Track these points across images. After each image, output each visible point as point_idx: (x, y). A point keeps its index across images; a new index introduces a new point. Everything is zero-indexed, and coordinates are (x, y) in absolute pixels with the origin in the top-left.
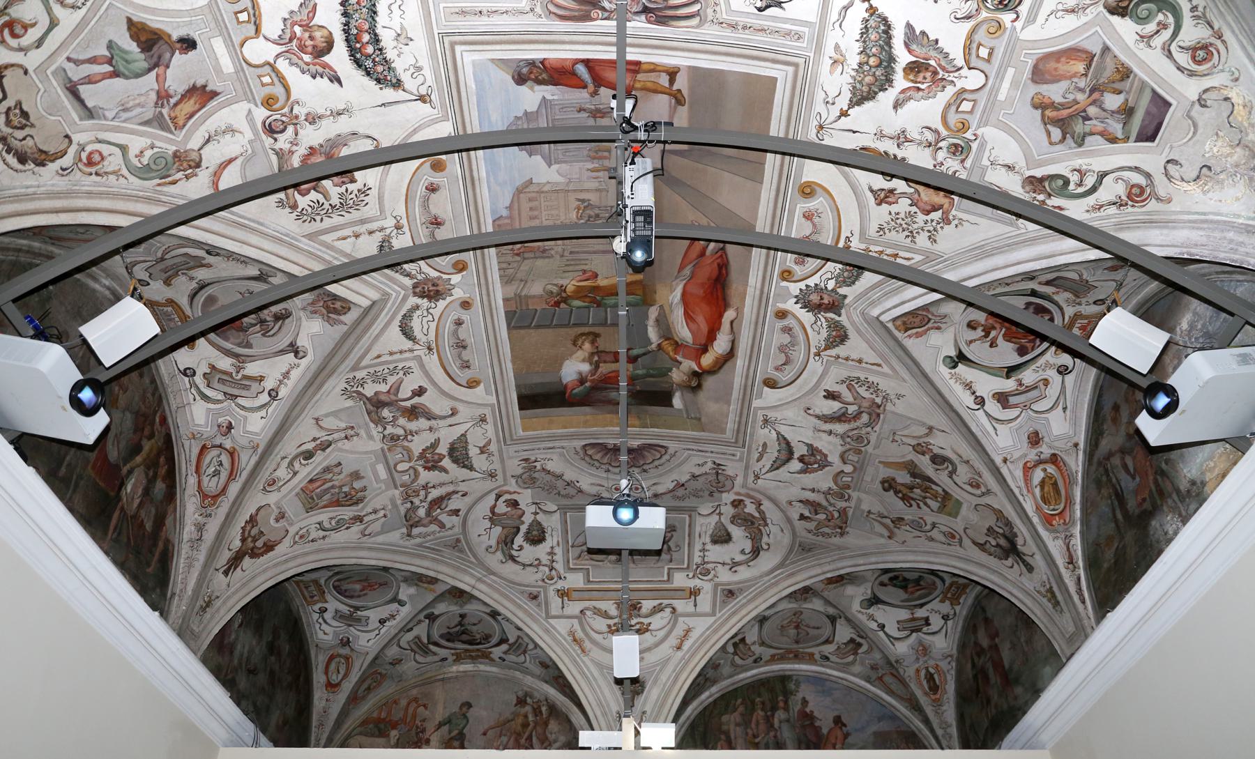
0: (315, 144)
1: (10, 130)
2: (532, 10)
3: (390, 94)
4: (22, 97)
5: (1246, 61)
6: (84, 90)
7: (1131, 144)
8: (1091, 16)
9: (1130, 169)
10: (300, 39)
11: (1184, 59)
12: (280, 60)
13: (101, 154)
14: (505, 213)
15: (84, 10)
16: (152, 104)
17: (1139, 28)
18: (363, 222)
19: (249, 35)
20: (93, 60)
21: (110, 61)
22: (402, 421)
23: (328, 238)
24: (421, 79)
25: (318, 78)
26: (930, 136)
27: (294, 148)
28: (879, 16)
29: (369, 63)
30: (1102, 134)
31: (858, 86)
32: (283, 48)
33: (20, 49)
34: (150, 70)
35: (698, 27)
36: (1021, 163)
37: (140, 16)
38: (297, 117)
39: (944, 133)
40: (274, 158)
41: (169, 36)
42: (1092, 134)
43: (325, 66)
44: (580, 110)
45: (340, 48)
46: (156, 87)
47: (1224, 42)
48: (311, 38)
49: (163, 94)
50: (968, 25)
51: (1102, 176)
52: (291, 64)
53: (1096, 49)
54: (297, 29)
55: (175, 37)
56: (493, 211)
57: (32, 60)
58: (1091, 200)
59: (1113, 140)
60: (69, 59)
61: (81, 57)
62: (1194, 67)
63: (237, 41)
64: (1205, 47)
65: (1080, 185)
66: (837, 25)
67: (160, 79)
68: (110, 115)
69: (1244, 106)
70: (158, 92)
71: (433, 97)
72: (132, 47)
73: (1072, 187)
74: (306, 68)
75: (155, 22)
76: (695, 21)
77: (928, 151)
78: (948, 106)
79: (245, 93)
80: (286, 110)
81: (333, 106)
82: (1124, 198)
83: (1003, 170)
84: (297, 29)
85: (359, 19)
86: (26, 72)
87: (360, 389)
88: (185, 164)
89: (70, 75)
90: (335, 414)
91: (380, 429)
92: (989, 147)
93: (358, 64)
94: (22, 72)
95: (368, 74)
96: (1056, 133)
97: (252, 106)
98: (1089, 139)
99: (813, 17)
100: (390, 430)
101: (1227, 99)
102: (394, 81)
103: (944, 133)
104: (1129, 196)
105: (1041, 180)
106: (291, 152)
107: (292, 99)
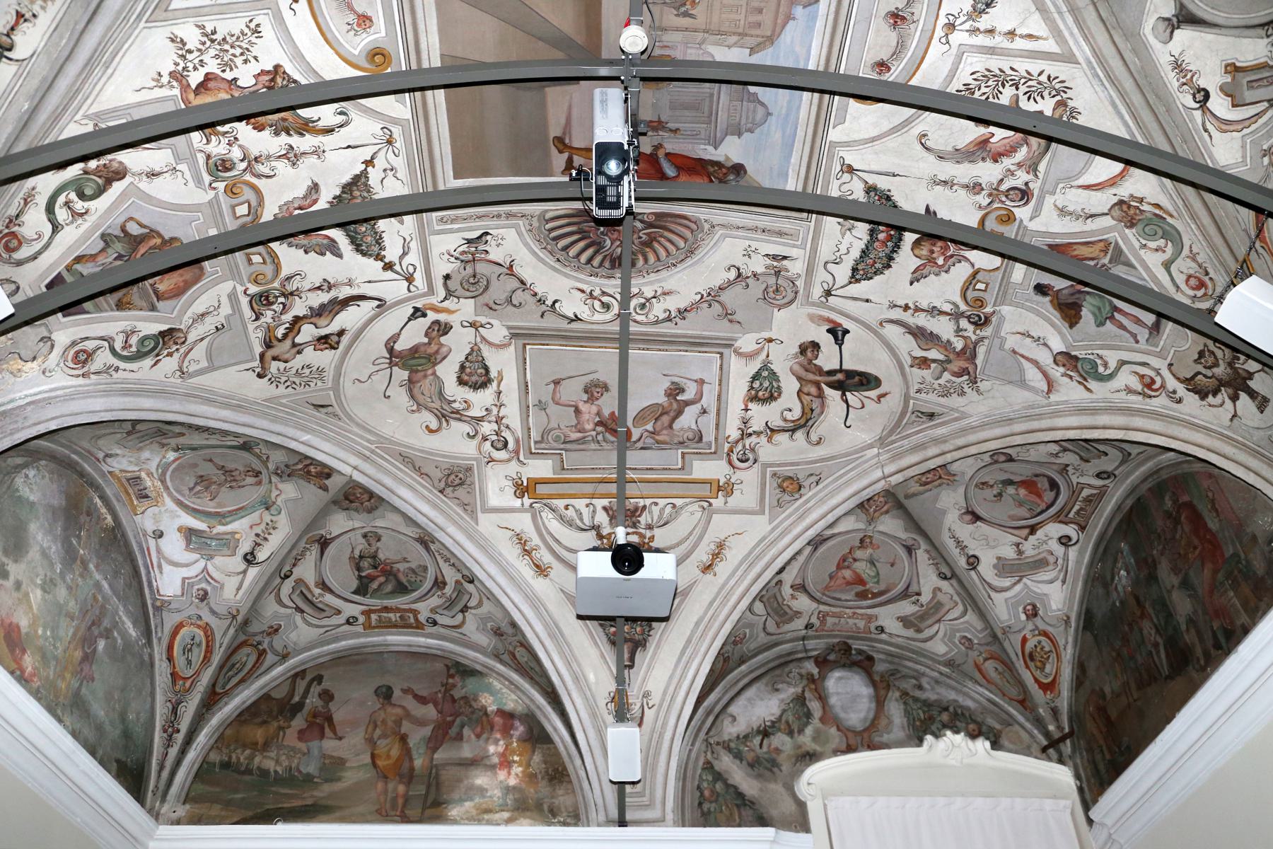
0: (989, 164)
1: (1221, 362)
2: (713, 227)
3: (883, 183)
5: (53, 386)
7: (61, 268)
8: (186, 318)
9: (39, 253)
10: (943, 254)
11: (90, 345)
13: (1187, 281)
14: (799, 11)
17: (141, 335)
18: (991, 51)
21: (1112, 318)
23: (1051, 46)
24: (844, 188)
26: (261, 168)
27: (1013, 168)
28: (371, 255)
30: (93, 257)
31: (365, 194)
35: (547, 211)
36: (144, 185)
37: (1063, 326)
38: (990, 195)
39: (248, 177)
40: (1042, 167)
41: (1051, 302)
42: (103, 250)
44: (676, 131)
47: (78, 376)
48: (932, 252)
50: (285, 272)
51: (56, 228)
53: (160, 305)
54: (940, 261)
55: (1048, 299)
56: (813, 18)
58: (42, 201)
59: (79, 259)
60: (1137, 342)
61: (1128, 335)
62: (77, 348)
63: (999, 274)
64: (85, 362)
65: (67, 204)
66: (408, 239)
69: (19, 370)
71: (839, 168)
72: (1085, 312)
73: (73, 196)
75: (1055, 316)
76: (548, 216)
77: (254, 152)
78: (261, 202)
80: (996, 205)
81: (947, 192)
82: (15, 229)
83: (158, 169)
84: (940, 261)
88: (1132, 212)
92: (191, 184)
96: (134, 229)
97: (1025, 223)
98: (101, 245)
99: (434, 240)
101: (34, 358)
102: (872, 194)
103: (248, 177)
104: (13, 234)
105: (109, 182)
106: (1019, 165)
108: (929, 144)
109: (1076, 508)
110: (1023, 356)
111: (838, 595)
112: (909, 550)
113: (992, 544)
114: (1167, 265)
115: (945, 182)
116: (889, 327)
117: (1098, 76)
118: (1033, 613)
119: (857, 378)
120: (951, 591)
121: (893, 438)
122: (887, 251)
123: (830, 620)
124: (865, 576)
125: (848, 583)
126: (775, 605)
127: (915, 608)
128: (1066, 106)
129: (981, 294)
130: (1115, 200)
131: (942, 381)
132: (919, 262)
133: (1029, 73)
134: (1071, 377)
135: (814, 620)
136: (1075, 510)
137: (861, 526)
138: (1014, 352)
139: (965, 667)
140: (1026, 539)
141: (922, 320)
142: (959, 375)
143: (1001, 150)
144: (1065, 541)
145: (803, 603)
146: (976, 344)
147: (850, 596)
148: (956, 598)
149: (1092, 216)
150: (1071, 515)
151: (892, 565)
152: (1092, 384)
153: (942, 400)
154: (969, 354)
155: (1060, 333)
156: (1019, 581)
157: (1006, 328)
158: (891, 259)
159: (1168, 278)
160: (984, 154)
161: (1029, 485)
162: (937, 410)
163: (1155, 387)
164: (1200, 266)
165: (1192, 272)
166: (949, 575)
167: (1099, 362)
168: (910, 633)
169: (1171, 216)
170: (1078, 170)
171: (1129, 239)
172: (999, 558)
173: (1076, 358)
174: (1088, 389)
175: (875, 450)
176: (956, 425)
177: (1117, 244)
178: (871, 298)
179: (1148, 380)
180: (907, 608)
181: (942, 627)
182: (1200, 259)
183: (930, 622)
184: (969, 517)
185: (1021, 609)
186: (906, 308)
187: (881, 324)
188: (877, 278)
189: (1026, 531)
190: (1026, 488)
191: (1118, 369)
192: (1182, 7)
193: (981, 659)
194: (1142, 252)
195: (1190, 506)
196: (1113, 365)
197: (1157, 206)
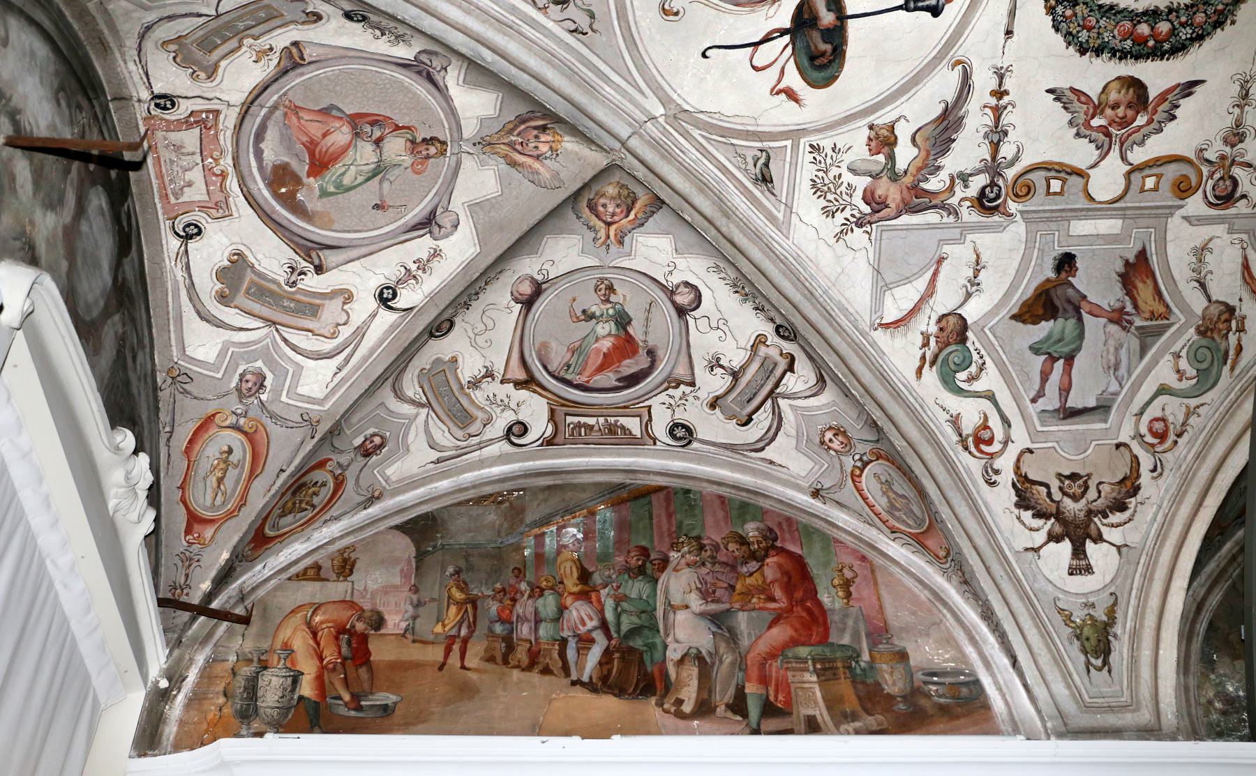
6: (1074, 401)
12: (1131, 157)
15: (987, 359)
16: (1123, 334)
19: (1081, 187)
21: (1056, 360)
25: (1177, 112)
29: (1185, 33)
33: (1005, 443)
34: (1080, 319)
37: (1014, 304)
38: (1223, 158)
41: (1048, 280)
43: (1163, 97)
48: (1115, 106)
49: (1115, 315)
52: (1142, 143)
54: (1096, 122)
55: (1052, 275)
57: (1021, 438)
60: (1034, 401)
61: (1037, 387)
63: (1082, 203)
67: (1096, 312)
68: (1114, 387)
70: (1111, 321)
72: (1045, 327)
74: (1154, 125)
75: (1026, 290)
79: (1157, 216)
81: (1229, 102)
84: (1096, 122)
85: (1112, 33)
86: (1030, 451)
93: (1179, 49)
94: (1027, 455)
95: (1200, 38)
97: (1182, 212)
107: (1192, 156)
109: (591, 421)
110: (935, 274)
111: (271, 135)
112: (428, 223)
113: (480, 340)
114: (1163, 390)
116: (955, 77)
118: (366, 452)
119: (828, 47)
120: (358, 318)
121: (696, 133)
122: (1116, 43)
123: (190, 138)
124: (338, 168)
125: (311, 146)
126: (241, 25)
127: (281, 275)
129: (1041, 189)
130: (1233, 302)
131: (848, 177)
132: (1094, 94)
134: (926, 344)
135: (184, 108)
136: (583, 420)
137: (469, 130)
138: (940, 261)
139: (188, 401)
140: (502, 382)
141: (976, 119)
142: (869, 197)
144: (517, 430)
145: (241, 74)
146: (943, 206)
147: (272, 152)
148: (346, 332)
149: (1203, 286)
150: (569, 419)
151: (377, 207)
152: (931, 375)
153: (804, 187)
154: (917, 200)
155: (997, 307)
156: (422, 405)
157: (985, 241)
158: (1098, 52)
159: (1147, 398)
161: (626, 345)
162: (781, 185)
163: (983, 447)
164: (1183, 424)
165: (1171, 419)
166: (400, 303)
167: (973, 369)
168: (207, 285)
169: (1232, 369)
171: (1181, 335)
172: (454, 360)
173: (963, 339)
174: (919, 372)
175: (662, 111)
176: (760, 222)
177: (1169, 326)
178: (1015, 38)
179: (986, 435)
180: (271, 257)
181: (259, 333)
182: (1193, 420)
183: (257, 308)
184: (527, 289)
185: (371, 431)
186: (999, 94)
187: (959, 62)
188: (1059, 38)
189: (521, 376)
190: (615, 347)
191: (977, 395)
193: (232, 420)
194: (1171, 358)
195: (799, 562)
196: (978, 386)
197: (1239, 349)
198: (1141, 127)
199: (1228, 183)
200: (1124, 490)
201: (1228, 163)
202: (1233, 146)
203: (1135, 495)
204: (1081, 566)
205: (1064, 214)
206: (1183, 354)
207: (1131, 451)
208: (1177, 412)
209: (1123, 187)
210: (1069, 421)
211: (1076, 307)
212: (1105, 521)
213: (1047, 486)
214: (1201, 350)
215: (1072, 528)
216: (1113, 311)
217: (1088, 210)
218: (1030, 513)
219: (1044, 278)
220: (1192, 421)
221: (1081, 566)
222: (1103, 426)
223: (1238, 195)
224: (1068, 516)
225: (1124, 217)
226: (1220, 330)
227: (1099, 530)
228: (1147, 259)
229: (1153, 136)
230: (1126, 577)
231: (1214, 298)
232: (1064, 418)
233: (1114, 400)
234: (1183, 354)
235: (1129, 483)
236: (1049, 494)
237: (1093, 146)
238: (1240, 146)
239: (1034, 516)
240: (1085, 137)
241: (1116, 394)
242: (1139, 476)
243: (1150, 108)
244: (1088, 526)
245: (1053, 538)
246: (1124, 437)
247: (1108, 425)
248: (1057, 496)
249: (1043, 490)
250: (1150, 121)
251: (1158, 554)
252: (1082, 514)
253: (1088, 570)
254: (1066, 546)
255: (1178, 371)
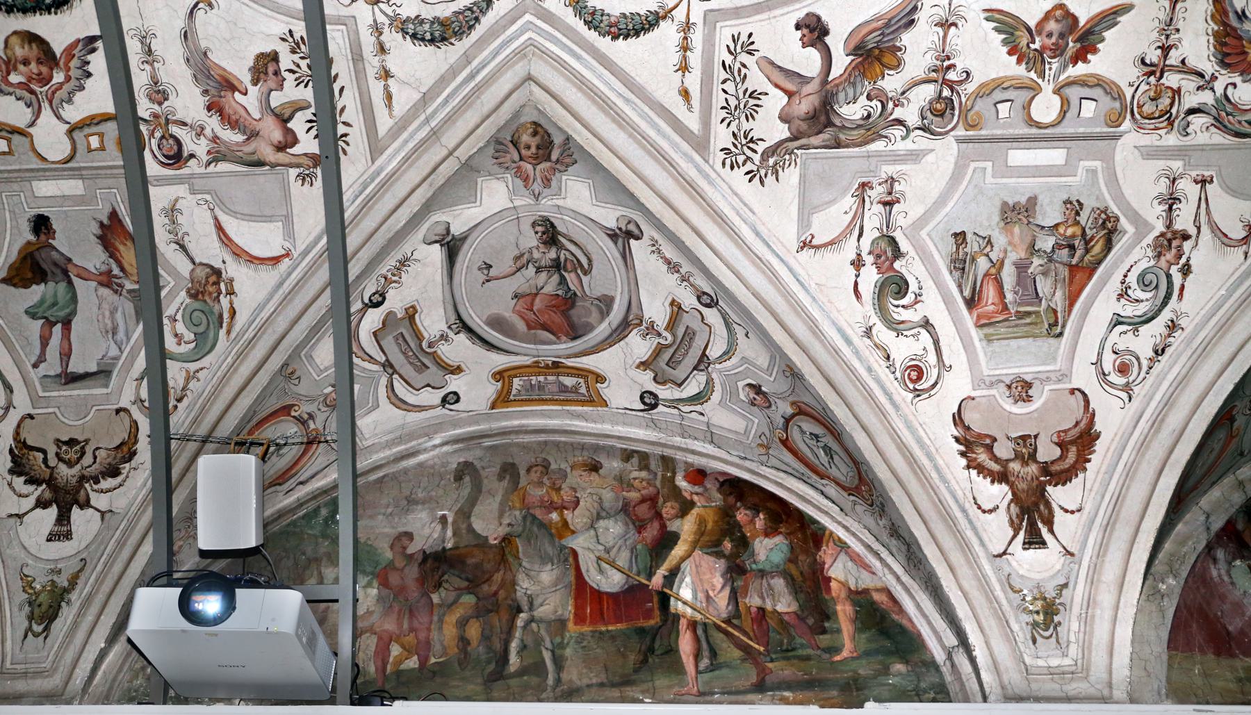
0: (201, 101)
4: (52, 436)
6: (76, 366)
10: (30, 79)
16: (116, 297)
18: (357, 58)
19: (28, 146)
20: (45, 341)
22: (891, 83)
23: (384, 123)
27: (208, 132)
32: (45, 105)
34: (70, 283)
40: (223, 167)
41: (29, 243)
45: (39, 24)
46: (94, 284)
49: (104, 279)
52: (70, 101)
55: (32, 238)
57: (22, 403)
60: (35, 366)
61: (38, 352)
63: (36, 164)
67: (85, 275)
68: (114, 351)
70: (101, 284)
72: (36, 292)
74: (73, 83)
84: (14, 78)
86: (31, 417)
87: (761, 147)
88: (211, 289)
89: (52, 373)
90: (806, 213)
91: (898, 132)
94: (28, 421)
100: (910, 114)
106: (215, 139)
108: (200, 14)
115: (150, 52)
117: (365, 189)
128: (315, 167)
130: (217, 264)
133: (342, 110)
143: (228, 110)
149: (183, 247)
160: (213, 91)
169: (229, 332)
170: (238, 209)
192: (463, 238)
197: (233, 312)
198: (61, 85)
199: (171, 141)
200: (119, 455)
201: (163, 121)
202: (160, 104)
203: (130, 460)
204: (61, 532)
205: (22, 175)
206: (179, 317)
207: (130, 416)
208: (177, 377)
209: (69, 147)
210: (71, 386)
211: (63, 270)
212: (95, 487)
213: (44, 452)
214: (196, 313)
215: (62, 494)
216: (101, 274)
217: (45, 170)
218: (22, 479)
219: (25, 241)
220: (191, 385)
221: (61, 532)
222: (104, 391)
223: (185, 154)
224: (61, 482)
225: (82, 177)
226: (210, 294)
227: (88, 495)
228: (120, 221)
229: (78, 94)
230: (102, 543)
231: (197, 261)
232: (66, 384)
233: (114, 365)
234: (179, 317)
235: (125, 449)
236: (45, 461)
237: (21, 103)
238: (166, 104)
239: (26, 482)
240: (11, 94)
241: (117, 358)
242: (136, 442)
243: (61, 63)
244: (78, 492)
245: (42, 504)
246: (124, 403)
247: (109, 390)
248: (53, 461)
249: (40, 456)
250: (68, 79)
251: (139, 519)
252: (74, 480)
253: (68, 536)
254: (53, 512)
255: (176, 335)
